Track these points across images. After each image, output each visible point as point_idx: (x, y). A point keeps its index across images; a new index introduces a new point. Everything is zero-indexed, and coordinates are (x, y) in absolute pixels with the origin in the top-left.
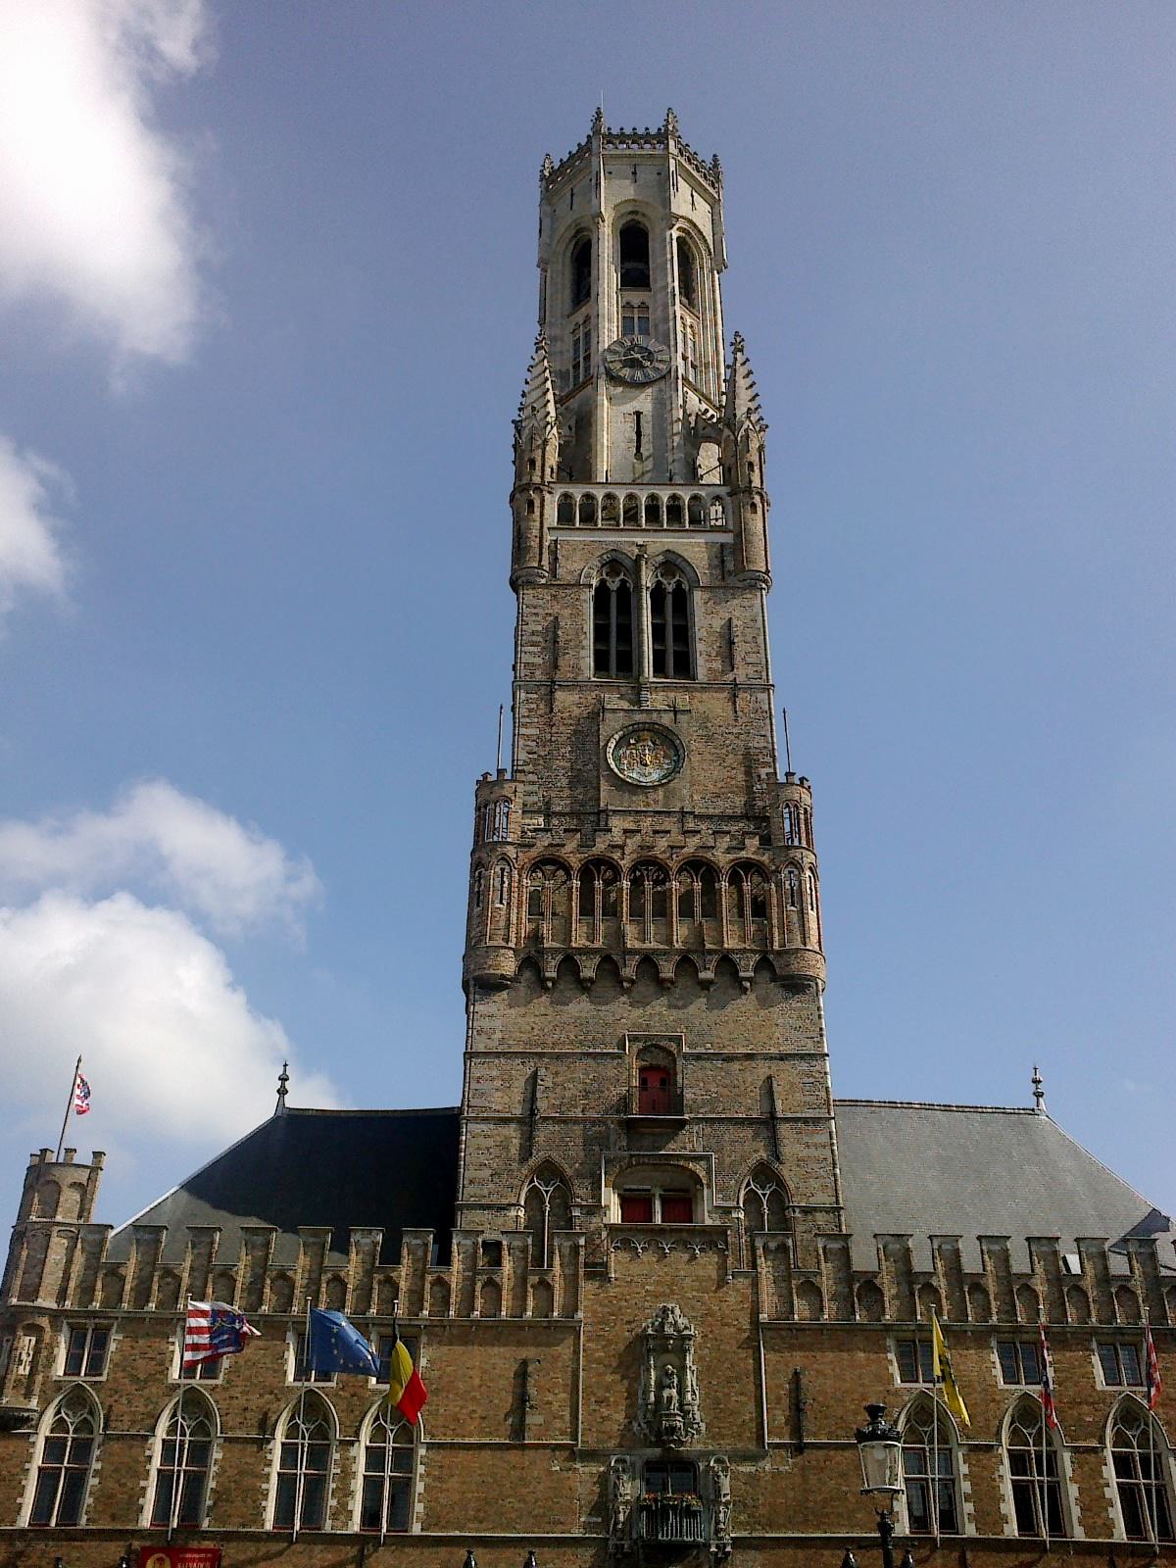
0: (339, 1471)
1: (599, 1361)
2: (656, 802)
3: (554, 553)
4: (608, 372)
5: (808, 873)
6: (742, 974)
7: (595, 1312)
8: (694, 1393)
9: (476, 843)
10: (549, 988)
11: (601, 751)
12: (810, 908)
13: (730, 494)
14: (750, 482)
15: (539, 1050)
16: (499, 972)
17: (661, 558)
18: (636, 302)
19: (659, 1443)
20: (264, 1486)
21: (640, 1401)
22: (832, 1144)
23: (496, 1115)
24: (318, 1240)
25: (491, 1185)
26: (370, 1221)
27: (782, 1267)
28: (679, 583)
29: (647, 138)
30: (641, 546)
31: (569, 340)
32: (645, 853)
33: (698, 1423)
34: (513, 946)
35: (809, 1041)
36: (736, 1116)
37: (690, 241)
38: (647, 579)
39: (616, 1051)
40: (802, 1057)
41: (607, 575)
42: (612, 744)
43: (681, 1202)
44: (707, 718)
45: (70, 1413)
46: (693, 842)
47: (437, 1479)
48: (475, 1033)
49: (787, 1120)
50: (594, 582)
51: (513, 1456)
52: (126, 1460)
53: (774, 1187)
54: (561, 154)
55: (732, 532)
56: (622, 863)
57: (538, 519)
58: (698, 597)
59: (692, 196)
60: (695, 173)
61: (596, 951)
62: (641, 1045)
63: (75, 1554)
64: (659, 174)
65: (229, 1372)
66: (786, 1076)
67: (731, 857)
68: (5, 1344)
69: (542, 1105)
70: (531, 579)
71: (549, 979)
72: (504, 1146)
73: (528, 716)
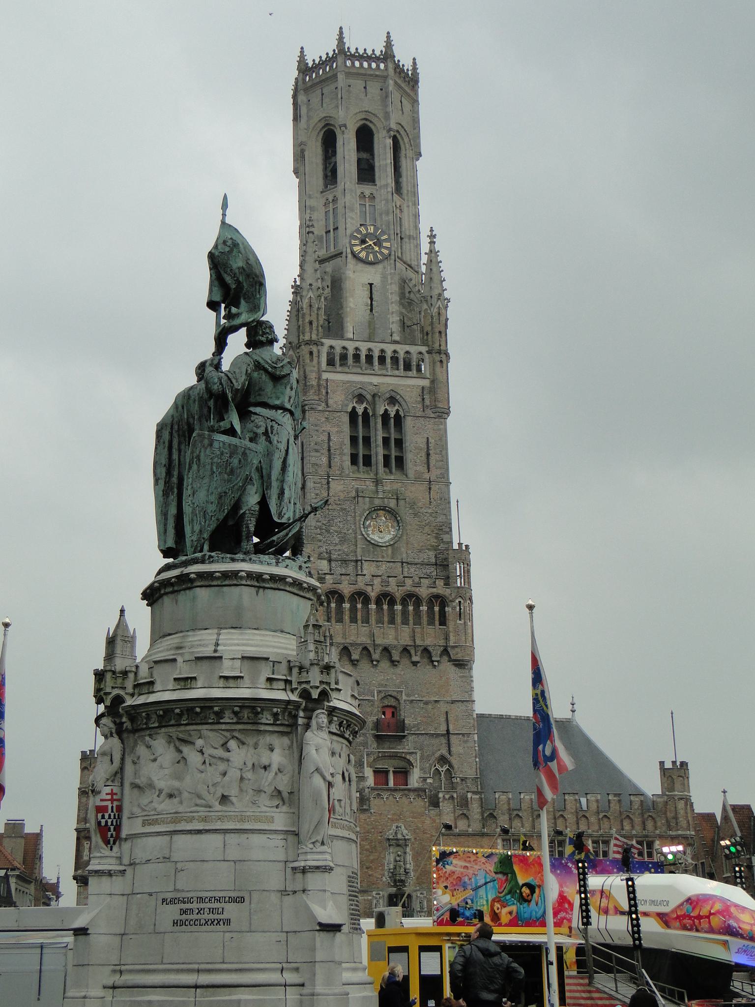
1: (367, 850)
2: (387, 555)
3: (327, 388)
4: (353, 253)
5: (469, 602)
6: (433, 659)
7: (365, 828)
13: (429, 352)
14: (440, 346)
17: (388, 395)
18: (367, 193)
19: (395, 886)
21: (386, 868)
22: (475, 747)
27: (452, 807)
28: (397, 411)
30: (376, 385)
31: (323, 210)
32: (384, 588)
36: (430, 732)
40: (462, 702)
43: (403, 774)
46: (409, 582)
49: (452, 734)
50: (349, 409)
53: (448, 767)
57: (317, 366)
58: (409, 424)
59: (401, 101)
60: (403, 85)
61: (361, 644)
62: (383, 695)
64: (381, 89)
66: (457, 711)
68: (85, 845)
70: (314, 406)
73: (316, 498)
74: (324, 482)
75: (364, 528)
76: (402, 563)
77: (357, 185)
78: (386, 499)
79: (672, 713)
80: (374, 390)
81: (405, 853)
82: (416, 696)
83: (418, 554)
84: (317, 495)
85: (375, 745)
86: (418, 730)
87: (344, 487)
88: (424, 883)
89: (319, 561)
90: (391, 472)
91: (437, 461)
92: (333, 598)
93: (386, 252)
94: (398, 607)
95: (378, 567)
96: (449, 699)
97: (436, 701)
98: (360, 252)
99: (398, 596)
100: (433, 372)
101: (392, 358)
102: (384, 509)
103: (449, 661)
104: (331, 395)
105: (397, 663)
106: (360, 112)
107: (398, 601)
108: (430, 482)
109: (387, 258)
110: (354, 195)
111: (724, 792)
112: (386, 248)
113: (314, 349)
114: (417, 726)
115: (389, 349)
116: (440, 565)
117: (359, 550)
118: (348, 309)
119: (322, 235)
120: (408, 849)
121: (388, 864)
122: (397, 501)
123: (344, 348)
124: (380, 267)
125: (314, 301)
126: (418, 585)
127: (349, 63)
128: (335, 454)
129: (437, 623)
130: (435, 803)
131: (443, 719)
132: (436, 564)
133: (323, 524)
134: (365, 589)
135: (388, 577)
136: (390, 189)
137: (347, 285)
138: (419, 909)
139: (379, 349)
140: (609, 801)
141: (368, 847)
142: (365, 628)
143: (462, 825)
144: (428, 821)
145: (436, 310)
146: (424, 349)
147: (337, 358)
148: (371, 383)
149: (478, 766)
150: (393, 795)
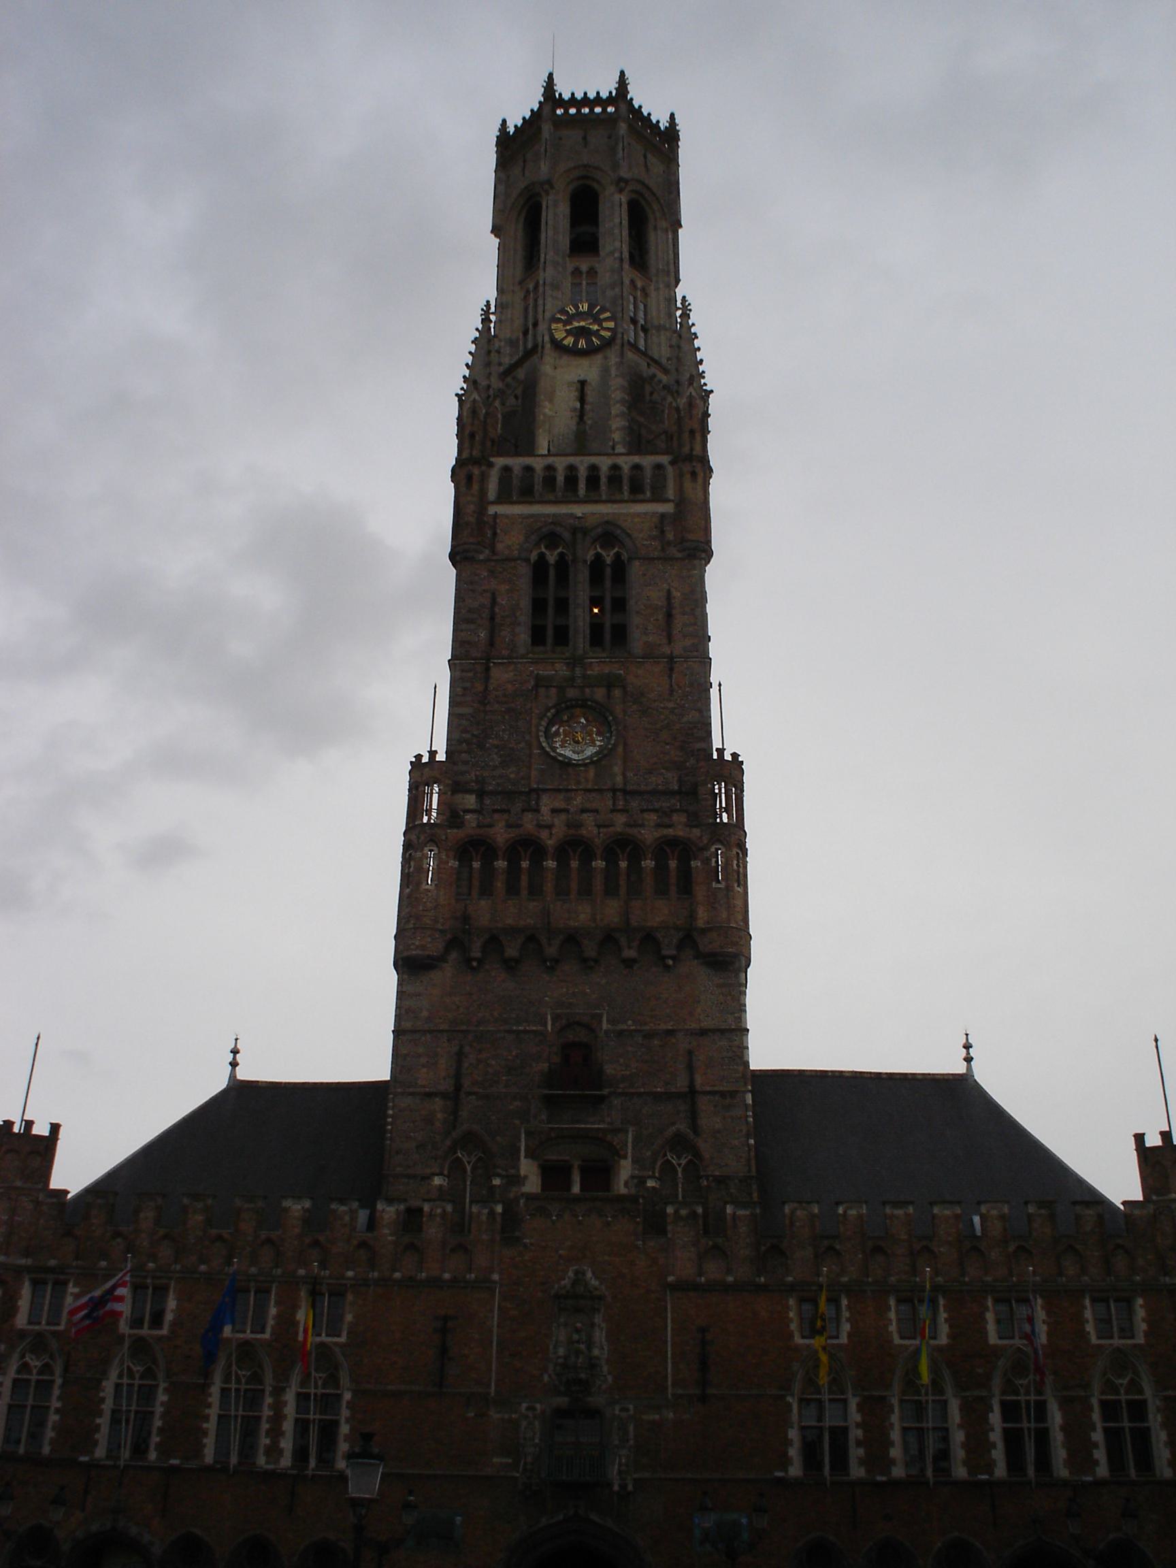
0: (271, 1413)
3: (494, 528)
8: (603, 1349)
9: (407, 824)
10: (473, 969)
11: (534, 729)
12: (736, 885)
13: (672, 463)
14: (692, 449)
15: (464, 1028)
16: (427, 953)
17: (599, 530)
18: (584, 268)
20: (205, 1425)
22: (747, 1116)
23: (422, 1090)
24: (252, 1206)
29: (598, 100)
30: (579, 518)
32: (572, 832)
33: (605, 1376)
34: (441, 928)
35: (729, 1016)
36: (655, 1090)
37: (643, 203)
39: (540, 1028)
40: (722, 1031)
41: (546, 548)
42: (544, 723)
45: (34, 1357)
46: (621, 819)
48: (403, 1011)
50: (534, 556)
53: (689, 1157)
54: (515, 121)
55: (673, 501)
56: (550, 842)
58: (636, 570)
59: (645, 157)
62: (564, 1021)
64: (610, 137)
65: (174, 1324)
67: (657, 835)
69: (466, 1083)
71: (475, 959)
73: (463, 695)
75: (546, 737)
77: (567, 259)
78: (587, 690)
79: (1156, 1040)
81: (593, 1325)
82: (630, 1022)
83: (645, 776)
84: (465, 689)
85: (544, 1117)
87: (515, 675)
89: (459, 797)
94: (599, 864)
96: (694, 1026)
97: (671, 1033)
98: (566, 337)
100: (680, 490)
102: (583, 704)
103: (696, 957)
105: (592, 964)
106: (575, 168)
108: (671, 658)
109: (608, 344)
110: (560, 269)
112: (608, 329)
113: (476, 471)
115: (604, 463)
117: (534, 773)
118: (542, 417)
119: (518, 339)
120: (598, 1319)
121: (555, 1347)
122: (609, 691)
123: (529, 469)
124: (599, 358)
127: (559, 112)
129: (673, 890)
130: (656, 1225)
132: (679, 792)
135: (583, 811)
136: (617, 255)
137: (543, 384)
138: (617, 1442)
139: (586, 465)
140: (1030, 1216)
142: (535, 904)
143: (713, 1270)
145: (684, 400)
146: (664, 459)
148: (572, 516)
149: (753, 1154)
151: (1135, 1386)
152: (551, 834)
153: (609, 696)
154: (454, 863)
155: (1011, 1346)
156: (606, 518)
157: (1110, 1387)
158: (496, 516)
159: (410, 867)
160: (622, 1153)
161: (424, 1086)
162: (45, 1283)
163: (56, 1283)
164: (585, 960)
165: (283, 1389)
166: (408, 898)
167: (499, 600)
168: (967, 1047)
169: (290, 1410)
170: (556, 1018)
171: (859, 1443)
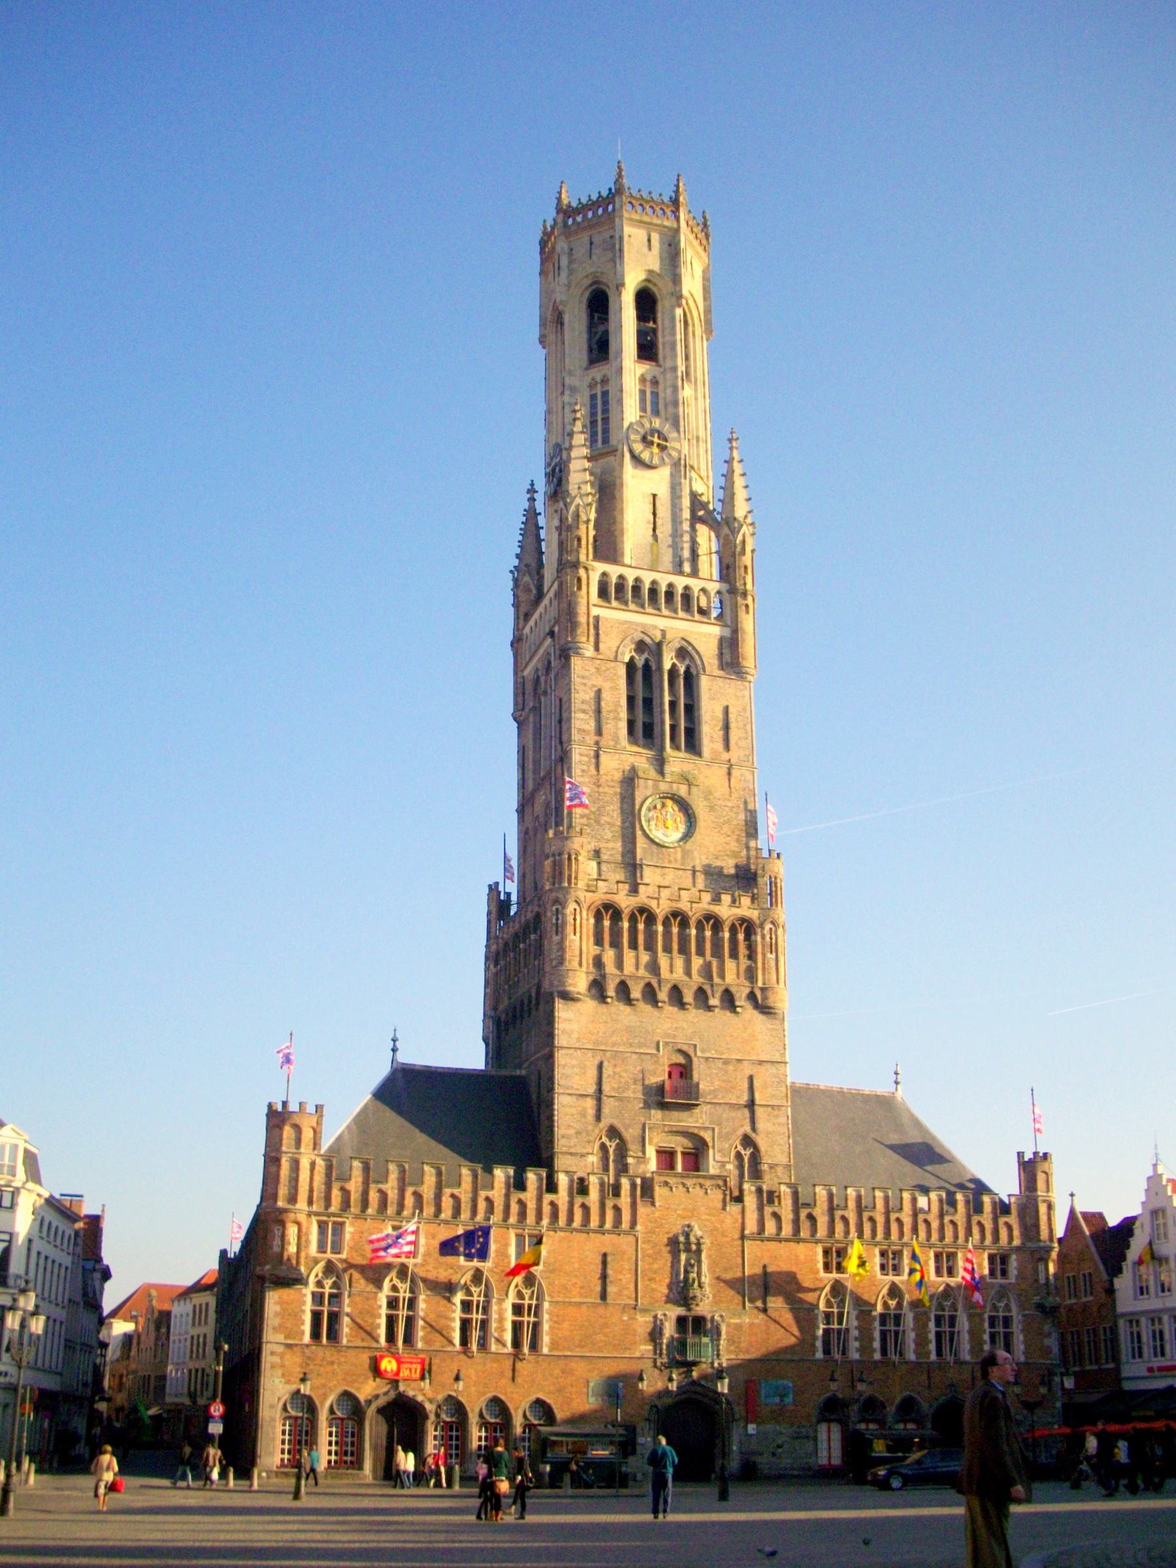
1: (649, 1256)
2: (676, 860)
3: (597, 628)
6: (737, 1003)
10: (607, 1003)
13: (729, 592)
14: (745, 584)
15: (603, 1048)
17: (678, 646)
25: (576, 1140)
26: (503, 1162)
32: (674, 905)
38: (667, 666)
44: (710, 793)
47: (556, 1322)
50: (627, 660)
51: (601, 1310)
52: (367, 1307)
56: (658, 911)
58: (704, 683)
61: (643, 978)
63: (343, 1360)
64: (670, 245)
65: (424, 1255)
67: (730, 913)
68: (276, 1231)
69: (606, 1088)
72: (583, 1115)
73: (582, 776)
74: (592, 753)
76: (694, 872)
78: (675, 786)
80: (658, 637)
84: (583, 771)
86: (715, 1097)
88: (721, 1301)
90: (678, 748)
91: (740, 738)
92: (607, 914)
93: (674, 454)
95: (663, 875)
96: (754, 1058)
97: (739, 1061)
98: (642, 452)
99: (694, 916)
101: (682, 595)
104: (602, 637)
107: (693, 922)
111: (1072, 1195)
114: (714, 1092)
116: (743, 878)
122: (690, 789)
123: (621, 577)
125: (581, 509)
126: (716, 900)
128: (608, 719)
131: (746, 1085)
133: (594, 813)
134: (648, 903)
135: (680, 889)
141: (650, 1252)
144: (729, 1221)
147: (612, 590)
148: (655, 627)
150: (684, 1185)
151: (1007, 1308)
152: (658, 904)
153: (689, 793)
154: (592, 921)
155: (943, 1282)
156: (681, 635)
157: (995, 1308)
158: (597, 618)
159: (557, 919)
160: (710, 1144)
161: (578, 1089)
162: (326, 1223)
163: (334, 1223)
164: (685, 1004)
165: (503, 1300)
166: (558, 943)
167: (604, 695)
168: (896, 1073)
169: (509, 1317)
170: (666, 1044)
171: (856, 1339)
